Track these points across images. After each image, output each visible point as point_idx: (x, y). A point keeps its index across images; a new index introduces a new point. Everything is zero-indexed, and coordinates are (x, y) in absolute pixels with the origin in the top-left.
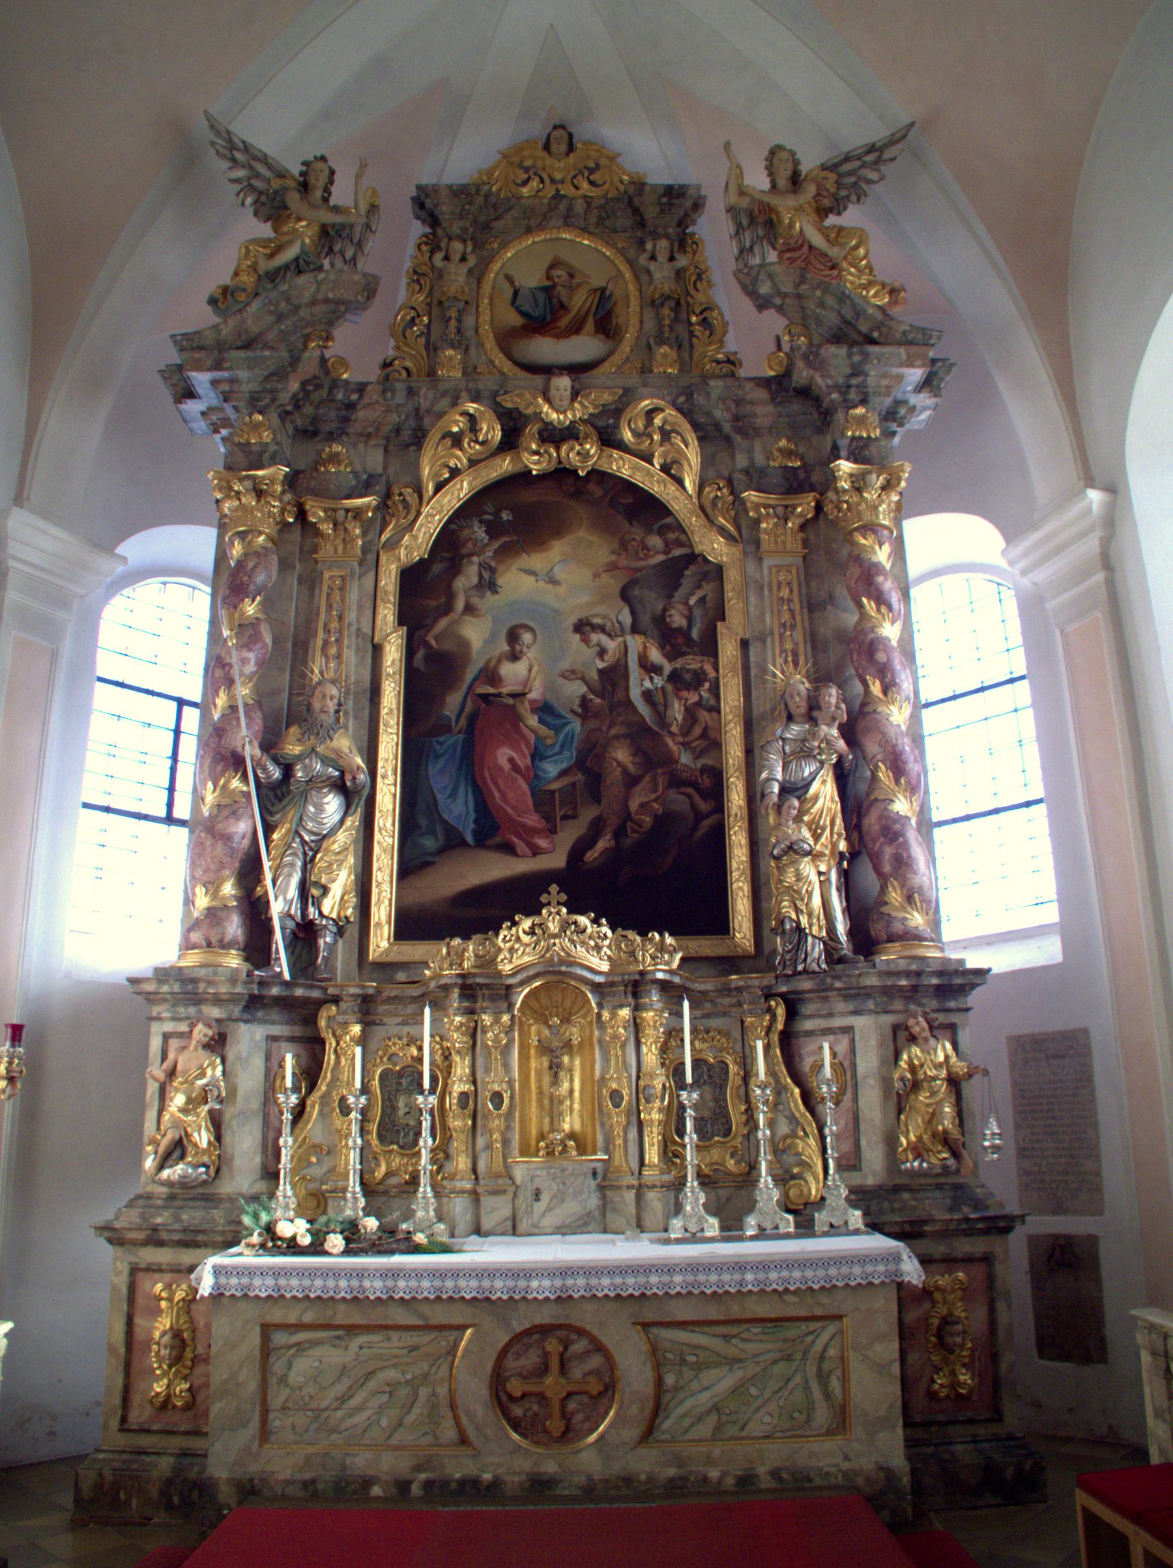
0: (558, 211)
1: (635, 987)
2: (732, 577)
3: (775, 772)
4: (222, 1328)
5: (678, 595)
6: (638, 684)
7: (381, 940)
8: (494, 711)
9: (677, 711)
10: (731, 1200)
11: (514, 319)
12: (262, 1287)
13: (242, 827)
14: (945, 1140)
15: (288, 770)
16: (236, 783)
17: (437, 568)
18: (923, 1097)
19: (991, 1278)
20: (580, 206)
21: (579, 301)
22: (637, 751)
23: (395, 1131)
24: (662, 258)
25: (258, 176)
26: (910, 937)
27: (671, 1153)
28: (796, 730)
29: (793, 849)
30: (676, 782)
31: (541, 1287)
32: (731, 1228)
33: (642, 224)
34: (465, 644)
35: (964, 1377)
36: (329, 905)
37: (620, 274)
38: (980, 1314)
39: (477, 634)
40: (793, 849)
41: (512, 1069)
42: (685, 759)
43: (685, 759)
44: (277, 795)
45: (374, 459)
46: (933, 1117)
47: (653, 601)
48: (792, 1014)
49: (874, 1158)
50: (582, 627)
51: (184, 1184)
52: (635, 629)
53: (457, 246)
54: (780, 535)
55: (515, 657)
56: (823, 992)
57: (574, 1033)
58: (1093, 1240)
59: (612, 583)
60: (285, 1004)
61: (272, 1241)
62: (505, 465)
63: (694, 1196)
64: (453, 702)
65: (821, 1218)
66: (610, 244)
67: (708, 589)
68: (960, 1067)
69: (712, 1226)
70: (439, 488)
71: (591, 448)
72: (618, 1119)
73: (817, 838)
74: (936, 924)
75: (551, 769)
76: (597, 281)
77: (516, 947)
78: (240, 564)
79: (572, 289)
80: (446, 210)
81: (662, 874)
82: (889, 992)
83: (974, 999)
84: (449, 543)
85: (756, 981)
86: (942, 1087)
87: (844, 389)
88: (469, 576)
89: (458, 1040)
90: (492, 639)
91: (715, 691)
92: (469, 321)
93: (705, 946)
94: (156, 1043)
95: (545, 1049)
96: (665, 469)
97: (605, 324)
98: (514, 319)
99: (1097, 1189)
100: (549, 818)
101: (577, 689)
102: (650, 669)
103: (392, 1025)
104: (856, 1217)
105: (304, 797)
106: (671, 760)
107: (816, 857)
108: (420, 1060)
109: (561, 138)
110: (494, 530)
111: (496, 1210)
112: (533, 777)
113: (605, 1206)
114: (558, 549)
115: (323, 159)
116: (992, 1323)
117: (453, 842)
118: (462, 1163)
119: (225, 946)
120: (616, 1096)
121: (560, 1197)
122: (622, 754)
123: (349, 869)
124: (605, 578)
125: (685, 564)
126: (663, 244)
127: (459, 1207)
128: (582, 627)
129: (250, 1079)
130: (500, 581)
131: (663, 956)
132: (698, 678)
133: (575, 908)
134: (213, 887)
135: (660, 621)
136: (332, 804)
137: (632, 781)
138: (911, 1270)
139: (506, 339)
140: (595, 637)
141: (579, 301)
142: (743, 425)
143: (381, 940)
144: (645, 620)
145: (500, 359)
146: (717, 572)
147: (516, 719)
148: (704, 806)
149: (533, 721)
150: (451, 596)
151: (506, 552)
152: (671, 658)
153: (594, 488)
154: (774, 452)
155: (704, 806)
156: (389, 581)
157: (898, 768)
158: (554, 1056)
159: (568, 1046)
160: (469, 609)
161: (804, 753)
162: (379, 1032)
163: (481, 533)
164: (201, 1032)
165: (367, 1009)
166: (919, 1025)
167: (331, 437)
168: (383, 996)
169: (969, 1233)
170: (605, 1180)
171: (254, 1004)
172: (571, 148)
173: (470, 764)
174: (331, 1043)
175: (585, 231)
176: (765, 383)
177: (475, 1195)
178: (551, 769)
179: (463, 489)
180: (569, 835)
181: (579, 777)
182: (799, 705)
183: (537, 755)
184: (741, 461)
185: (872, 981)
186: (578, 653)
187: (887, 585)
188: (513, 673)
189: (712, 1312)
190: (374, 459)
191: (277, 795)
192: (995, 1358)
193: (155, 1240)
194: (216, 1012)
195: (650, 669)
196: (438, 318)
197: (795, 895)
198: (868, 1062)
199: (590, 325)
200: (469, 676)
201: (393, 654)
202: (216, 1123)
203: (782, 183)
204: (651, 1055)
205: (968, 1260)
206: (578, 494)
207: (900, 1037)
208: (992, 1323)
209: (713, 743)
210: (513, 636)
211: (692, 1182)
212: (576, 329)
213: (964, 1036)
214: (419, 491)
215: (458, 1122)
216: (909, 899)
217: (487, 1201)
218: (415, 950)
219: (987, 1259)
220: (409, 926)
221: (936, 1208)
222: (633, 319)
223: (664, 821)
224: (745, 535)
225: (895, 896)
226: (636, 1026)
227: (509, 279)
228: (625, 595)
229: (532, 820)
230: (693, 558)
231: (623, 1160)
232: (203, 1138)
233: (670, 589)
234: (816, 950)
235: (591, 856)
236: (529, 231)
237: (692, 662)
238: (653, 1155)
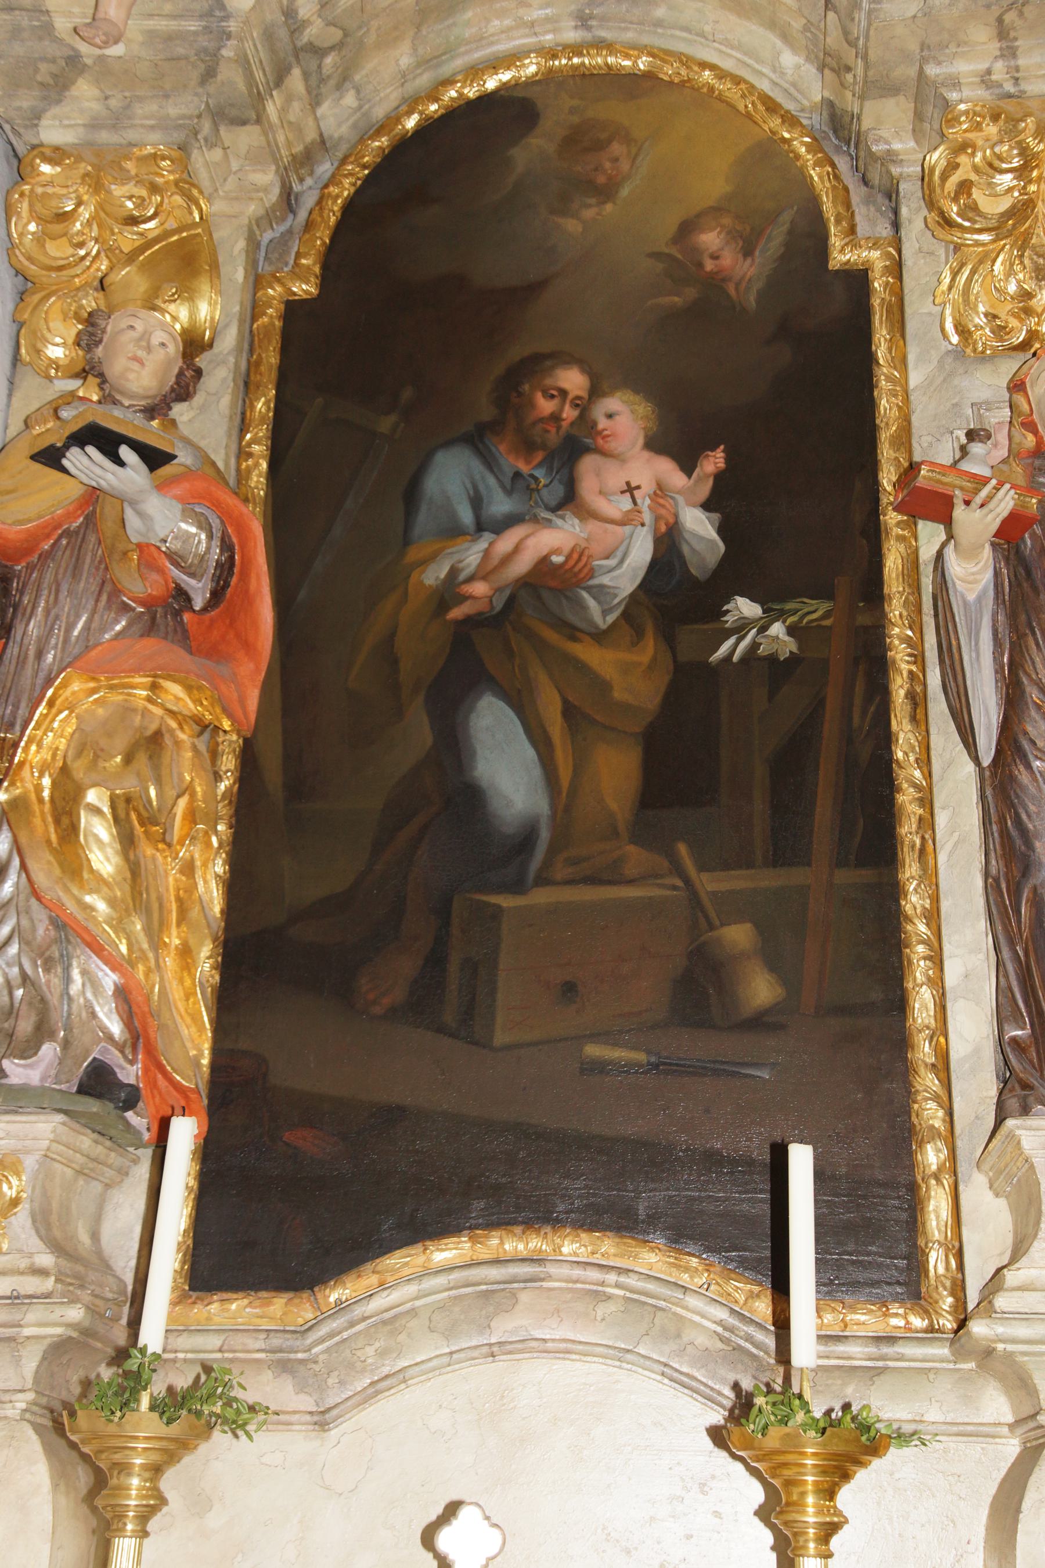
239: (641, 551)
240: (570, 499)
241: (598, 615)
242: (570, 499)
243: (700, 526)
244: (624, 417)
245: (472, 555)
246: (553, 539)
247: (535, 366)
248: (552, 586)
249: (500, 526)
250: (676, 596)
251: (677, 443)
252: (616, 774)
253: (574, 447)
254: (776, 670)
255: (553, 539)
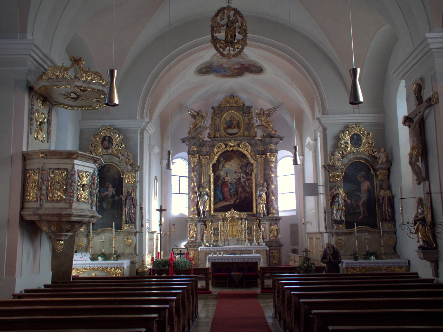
0: (232, 108)
1: (241, 219)
2: (255, 165)
3: (258, 193)
4: (200, 254)
5: (248, 168)
6: (242, 180)
7: (212, 212)
8: (225, 184)
9: (247, 184)
10: (251, 241)
11: (226, 126)
12: (205, 250)
13: (196, 200)
14: (275, 236)
15: (201, 193)
16: (195, 195)
17: (217, 164)
18: (273, 232)
19: (280, 251)
20: (235, 108)
21: (235, 123)
22: (242, 189)
23: (216, 235)
24: (246, 116)
25: (191, 112)
26: (274, 213)
27: (245, 237)
28: (261, 188)
29: (260, 203)
30: (247, 193)
31: (232, 249)
32: (251, 245)
33: (244, 110)
34: (221, 175)
35: (276, 261)
36: (207, 209)
37: (240, 118)
38: (278, 255)
39: (222, 173)
40: (260, 203)
41: (228, 228)
42: (248, 190)
43: (248, 190)
44: (201, 196)
45: (208, 149)
46: (274, 234)
47: (244, 169)
48: (260, 221)
49: (268, 238)
50: (235, 172)
51: (193, 241)
52: (242, 173)
53: (218, 116)
54: (260, 160)
55: (227, 176)
56: (263, 220)
57: (235, 224)
58: (297, 249)
59: (239, 166)
60: (203, 221)
61: (205, 246)
62: (225, 149)
63: (247, 241)
64: (219, 183)
65: (260, 244)
66: (239, 113)
67: (251, 167)
68: (277, 228)
69: (249, 244)
70: (217, 153)
71: (237, 147)
72: (239, 233)
73: (262, 201)
74: (278, 212)
75: (232, 191)
76: (237, 119)
77: (228, 214)
78: (193, 167)
79: (234, 121)
80: (216, 109)
81: (245, 205)
82: (270, 220)
83: (280, 221)
84: (218, 160)
85: (255, 218)
86: (275, 230)
87: (269, 142)
88: (221, 166)
89: (222, 225)
90: (224, 174)
91: (252, 181)
92: (220, 127)
93: (249, 213)
94: (188, 226)
95: (232, 225)
96: (246, 150)
97: (239, 127)
98: (226, 126)
99: (298, 243)
100: (231, 197)
101: (235, 181)
102: (244, 178)
103: (214, 223)
104: (264, 244)
105: (203, 196)
106: (246, 190)
107: (262, 204)
108: (218, 226)
109: (232, 96)
110: (224, 159)
111: (227, 243)
112: (230, 192)
113: (238, 243)
114: (232, 161)
115: (200, 110)
116: (280, 256)
117: (220, 200)
118: (223, 238)
119: (195, 214)
120: (239, 231)
121: (233, 242)
122: (240, 189)
123: (208, 205)
124: (238, 166)
125: (249, 164)
126: (247, 115)
127: (223, 242)
128: (235, 172)
129: (199, 229)
130: (225, 166)
131: (244, 215)
132: (250, 179)
133: (235, 210)
134: (194, 208)
135: (245, 171)
136: (206, 197)
137: (241, 193)
138: (268, 248)
139: (225, 129)
140: (237, 174)
141: (235, 123)
142: (256, 144)
143: (212, 212)
144: (243, 171)
145: (224, 133)
146: (252, 165)
147: (227, 185)
148: (250, 196)
149: (229, 185)
150: (219, 168)
151: (226, 162)
152: (247, 176)
153: (237, 153)
154: (261, 148)
155: (250, 196)
156: (211, 166)
157: (273, 193)
158: (232, 226)
159: (234, 225)
160: (221, 170)
161: (262, 191)
162: (213, 224)
163: (222, 159)
164: (194, 224)
165: (212, 221)
166: (273, 224)
167: (203, 146)
168: (213, 219)
169: (277, 246)
170: (238, 240)
171: (199, 221)
172: (234, 98)
173: (222, 190)
174: (208, 225)
175: (236, 111)
176: (259, 140)
177: (224, 241)
178: (232, 191)
179: (220, 153)
180: (234, 199)
181: (235, 192)
182: (261, 185)
183: (230, 189)
184: (256, 149)
185: (268, 218)
186: (235, 176)
187: (273, 169)
188: (227, 179)
189: (248, 252)
190: (208, 149)
191: (201, 196)
192: (280, 260)
193: (190, 247)
194: (195, 222)
195: (244, 178)
196: (215, 127)
197: (260, 208)
198: (267, 228)
199: (236, 127)
200: (221, 179)
201: (212, 175)
202: (196, 234)
203: (262, 113)
204: (243, 226)
205: (277, 249)
206: (235, 154)
207: (271, 225)
208: (280, 256)
209: (251, 188)
210: (227, 174)
211: (247, 240)
212: (234, 128)
213: (278, 225)
214: (214, 153)
215: (222, 234)
216: (273, 209)
217: (226, 242)
218: (216, 214)
219: (279, 249)
220: (215, 210)
221: (274, 244)
222: (242, 126)
223: (245, 198)
224: (256, 160)
225: (272, 209)
226: (242, 223)
227: (225, 119)
228: (241, 168)
229: (229, 198)
230: (250, 163)
231: (240, 237)
232: (195, 236)
233: (246, 167)
234: (262, 215)
235: (237, 202)
236: (228, 111)
237: (249, 177)
238: (243, 237)
239: (111, 194)
240: (108, 191)
241: (109, 197)
242: (108, 191)
243: (114, 192)
244: (110, 186)
245: (103, 194)
246: (107, 193)
247: (106, 182)
248: (107, 196)
249: (104, 192)
250: (113, 196)
251: (113, 187)
252: (110, 206)
253: (108, 187)
254: (118, 200)
255: (107, 193)
